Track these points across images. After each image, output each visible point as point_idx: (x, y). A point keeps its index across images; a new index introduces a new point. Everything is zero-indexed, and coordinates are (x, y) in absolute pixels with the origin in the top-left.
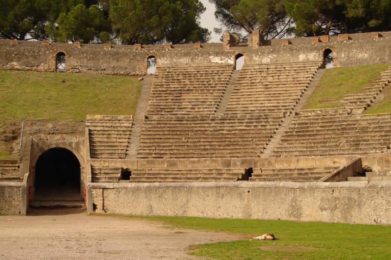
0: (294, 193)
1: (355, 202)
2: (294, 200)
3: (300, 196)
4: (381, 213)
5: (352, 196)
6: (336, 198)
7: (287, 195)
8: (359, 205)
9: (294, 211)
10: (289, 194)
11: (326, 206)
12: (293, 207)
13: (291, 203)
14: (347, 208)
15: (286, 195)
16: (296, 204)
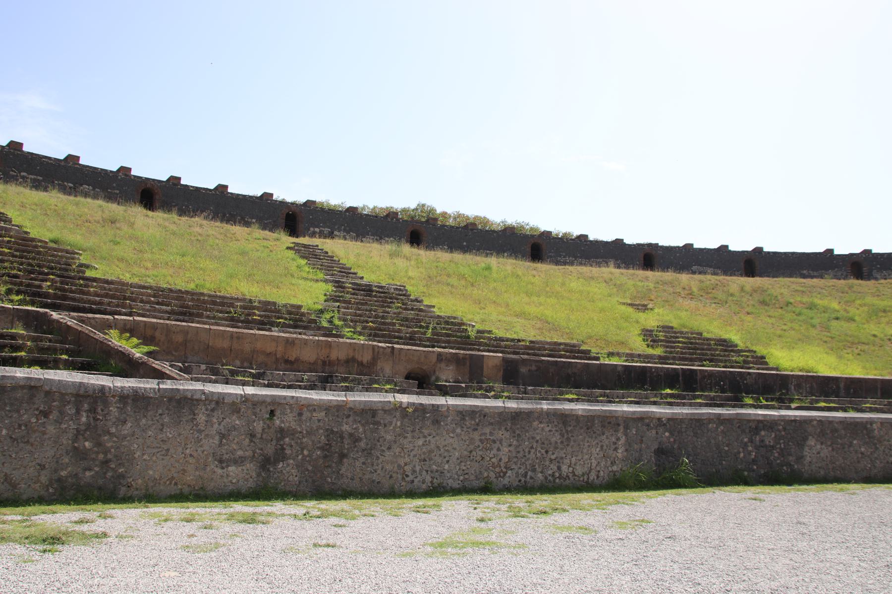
0: (93, 410)
1: (358, 440)
2: (94, 430)
3: (124, 422)
4: (446, 467)
5: (346, 428)
6: (281, 430)
7: (54, 416)
8: (368, 452)
9: (85, 469)
10: (62, 413)
11: (240, 453)
12: (79, 454)
13: (76, 439)
14: (325, 457)
15: (46, 414)
16: (99, 444)
